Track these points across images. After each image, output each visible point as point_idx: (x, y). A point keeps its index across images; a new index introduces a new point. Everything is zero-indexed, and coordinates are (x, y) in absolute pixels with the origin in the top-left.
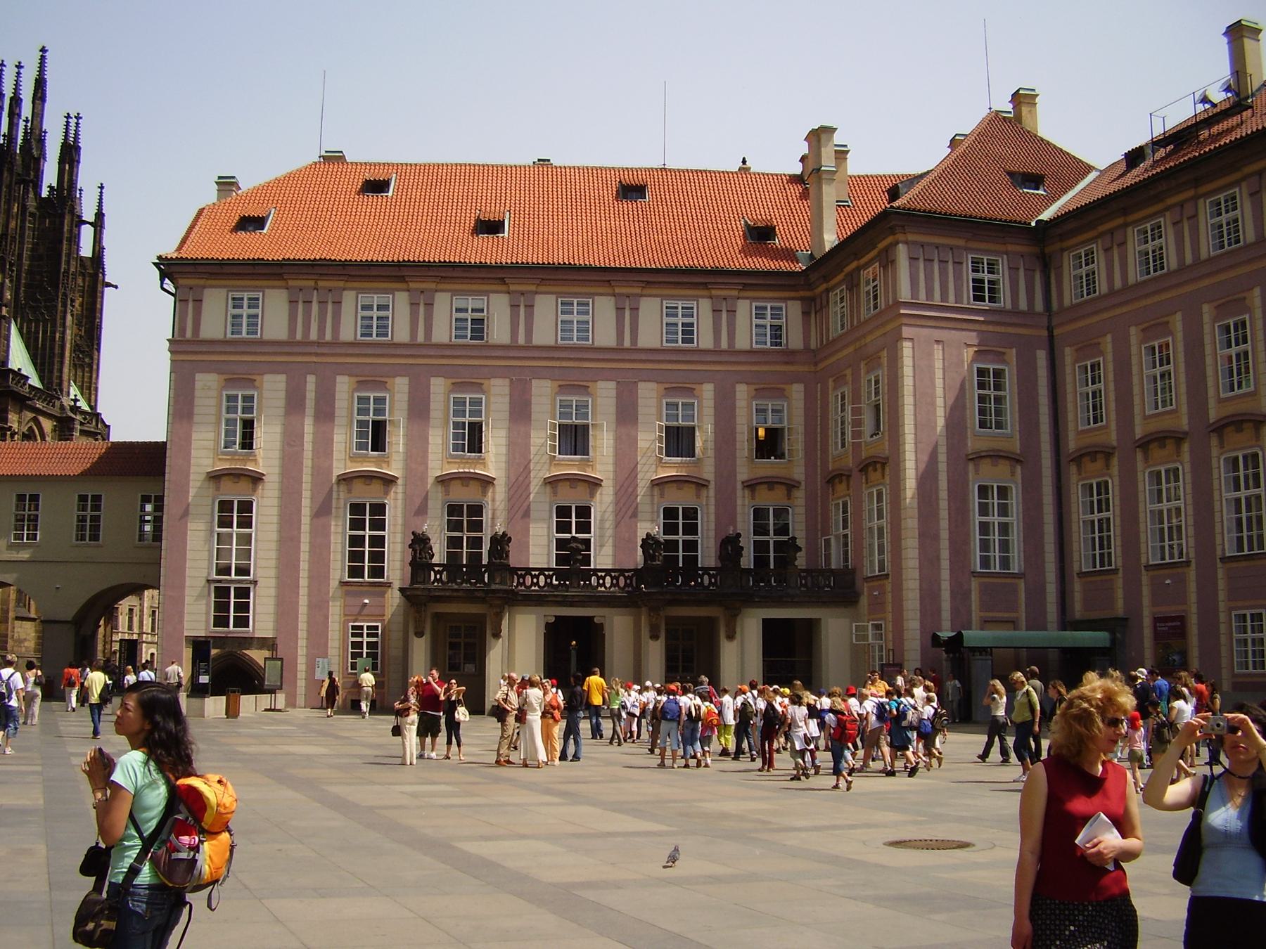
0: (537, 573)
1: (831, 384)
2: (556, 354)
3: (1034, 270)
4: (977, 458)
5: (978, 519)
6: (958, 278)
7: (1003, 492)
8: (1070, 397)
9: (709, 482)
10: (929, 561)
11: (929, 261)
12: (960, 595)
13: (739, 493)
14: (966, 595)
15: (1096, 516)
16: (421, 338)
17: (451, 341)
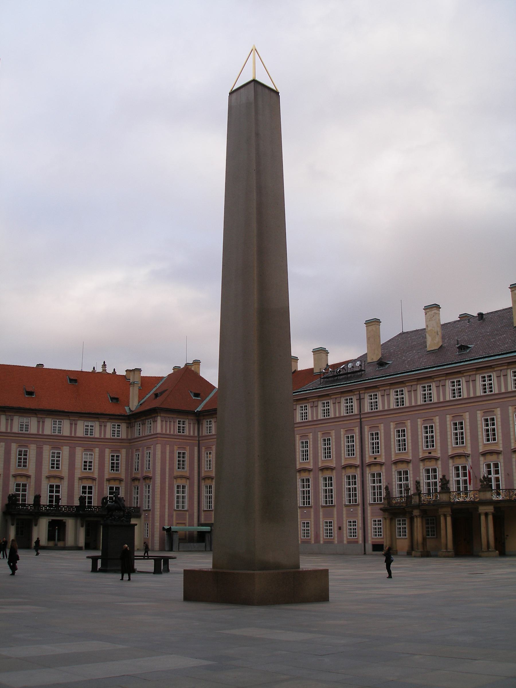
0: (42, 506)
1: (134, 450)
2: (51, 437)
3: (195, 424)
4: (176, 478)
5: (176, 495)
6: (174, 426)
7: (184, 487)
8: (203, 461)
9: (96, 478)
10: (162, 507)
11: (166, 421)
12: (170, 516)
13: (105, 482)
14: (172, 516)
15: (208, 495)
16: (9, 431)
17: (18, 431)
